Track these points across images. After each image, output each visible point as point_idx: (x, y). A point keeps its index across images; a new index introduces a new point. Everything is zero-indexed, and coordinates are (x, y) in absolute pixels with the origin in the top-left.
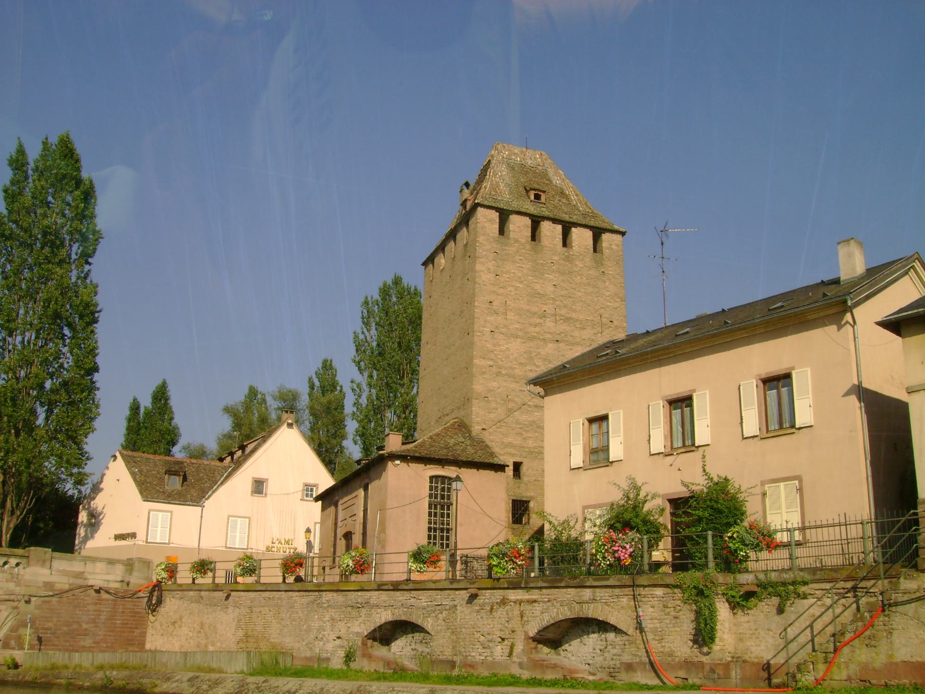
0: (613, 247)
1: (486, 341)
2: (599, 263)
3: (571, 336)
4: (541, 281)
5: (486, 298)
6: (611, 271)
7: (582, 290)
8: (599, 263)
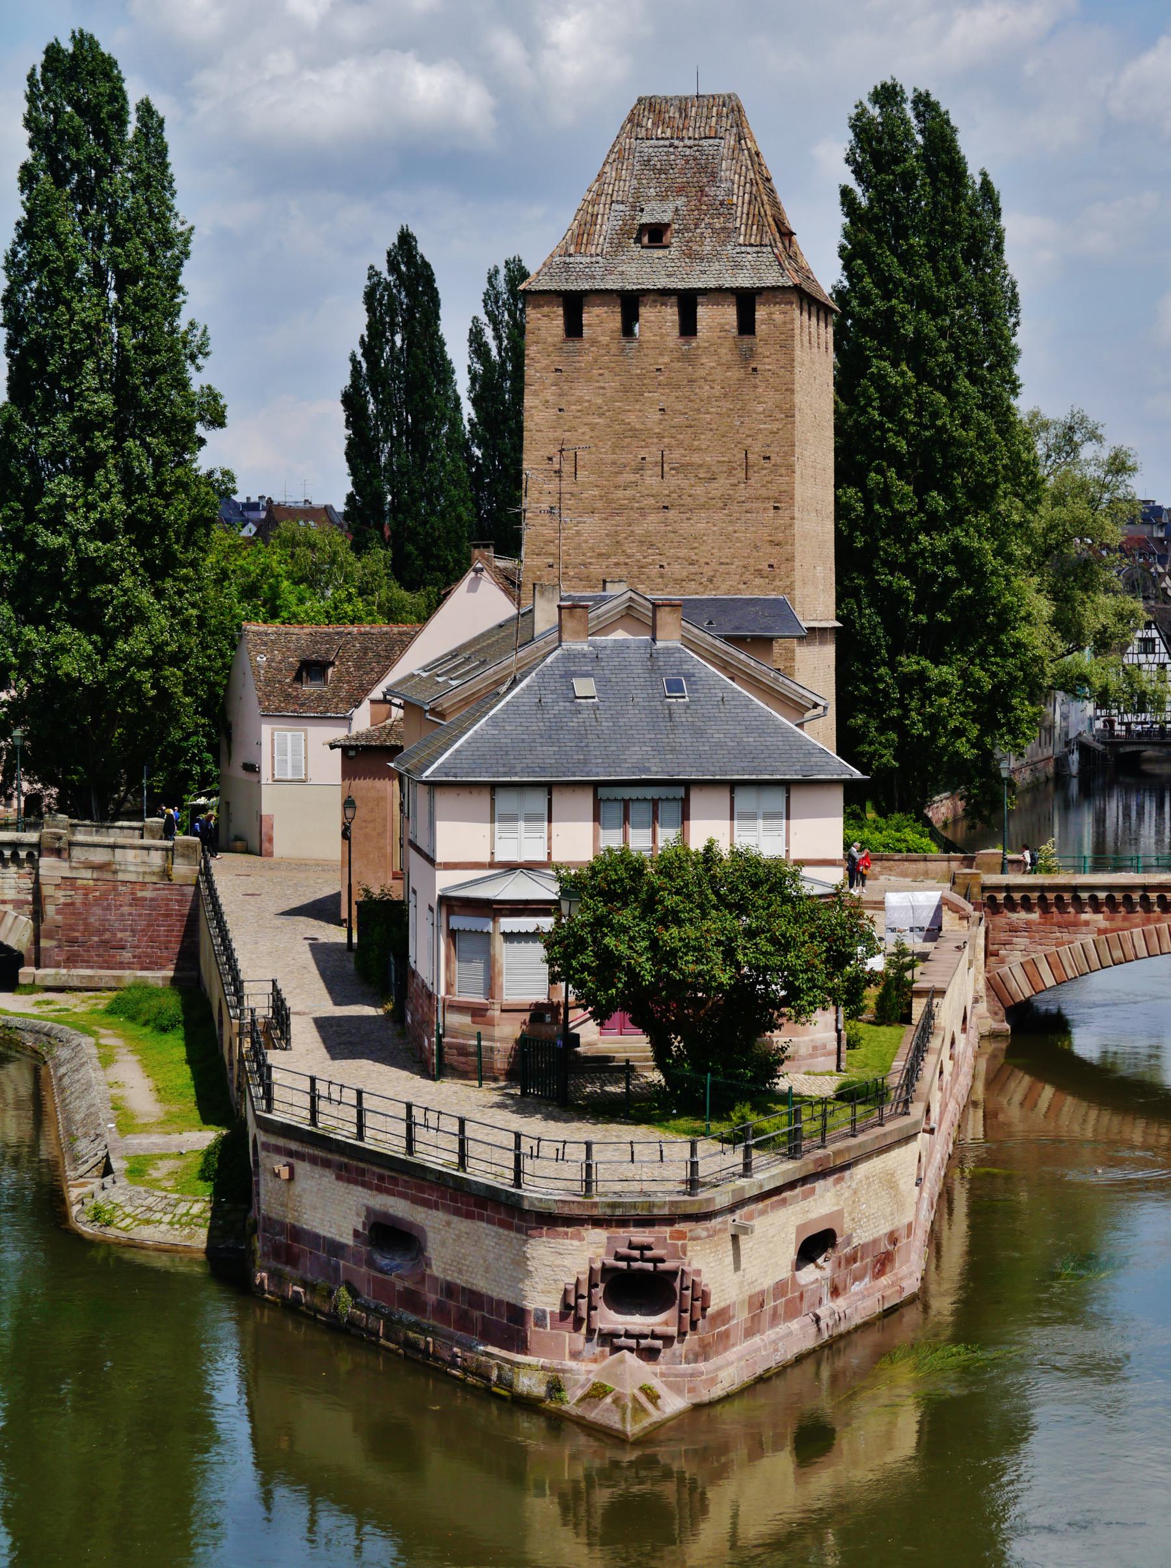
1: (542, 525)
2: (747, 357)
8: (747, 357)
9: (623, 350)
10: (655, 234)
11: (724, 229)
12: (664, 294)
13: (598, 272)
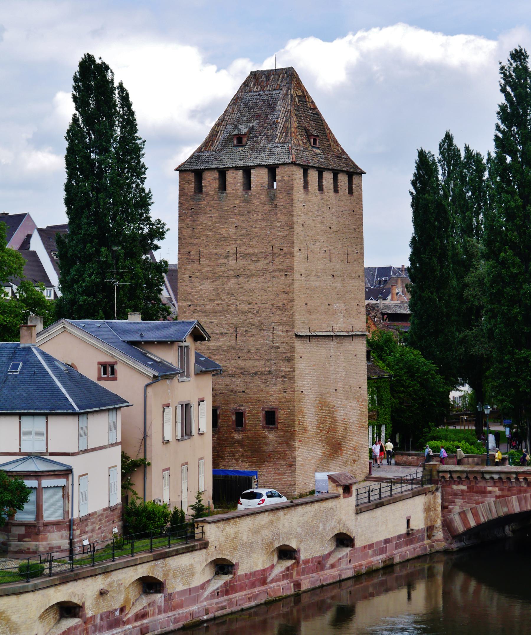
0: (286, 178)
1: (186, 286)
3: (248, 269)
4: (226, 226)
5: (185, 250)
6: (282, 202)
7: (258, 226)
9: (219, 198)
10: (240, 140)
11: (271, 135)
12: (237, 168)
13: (211, 159)
